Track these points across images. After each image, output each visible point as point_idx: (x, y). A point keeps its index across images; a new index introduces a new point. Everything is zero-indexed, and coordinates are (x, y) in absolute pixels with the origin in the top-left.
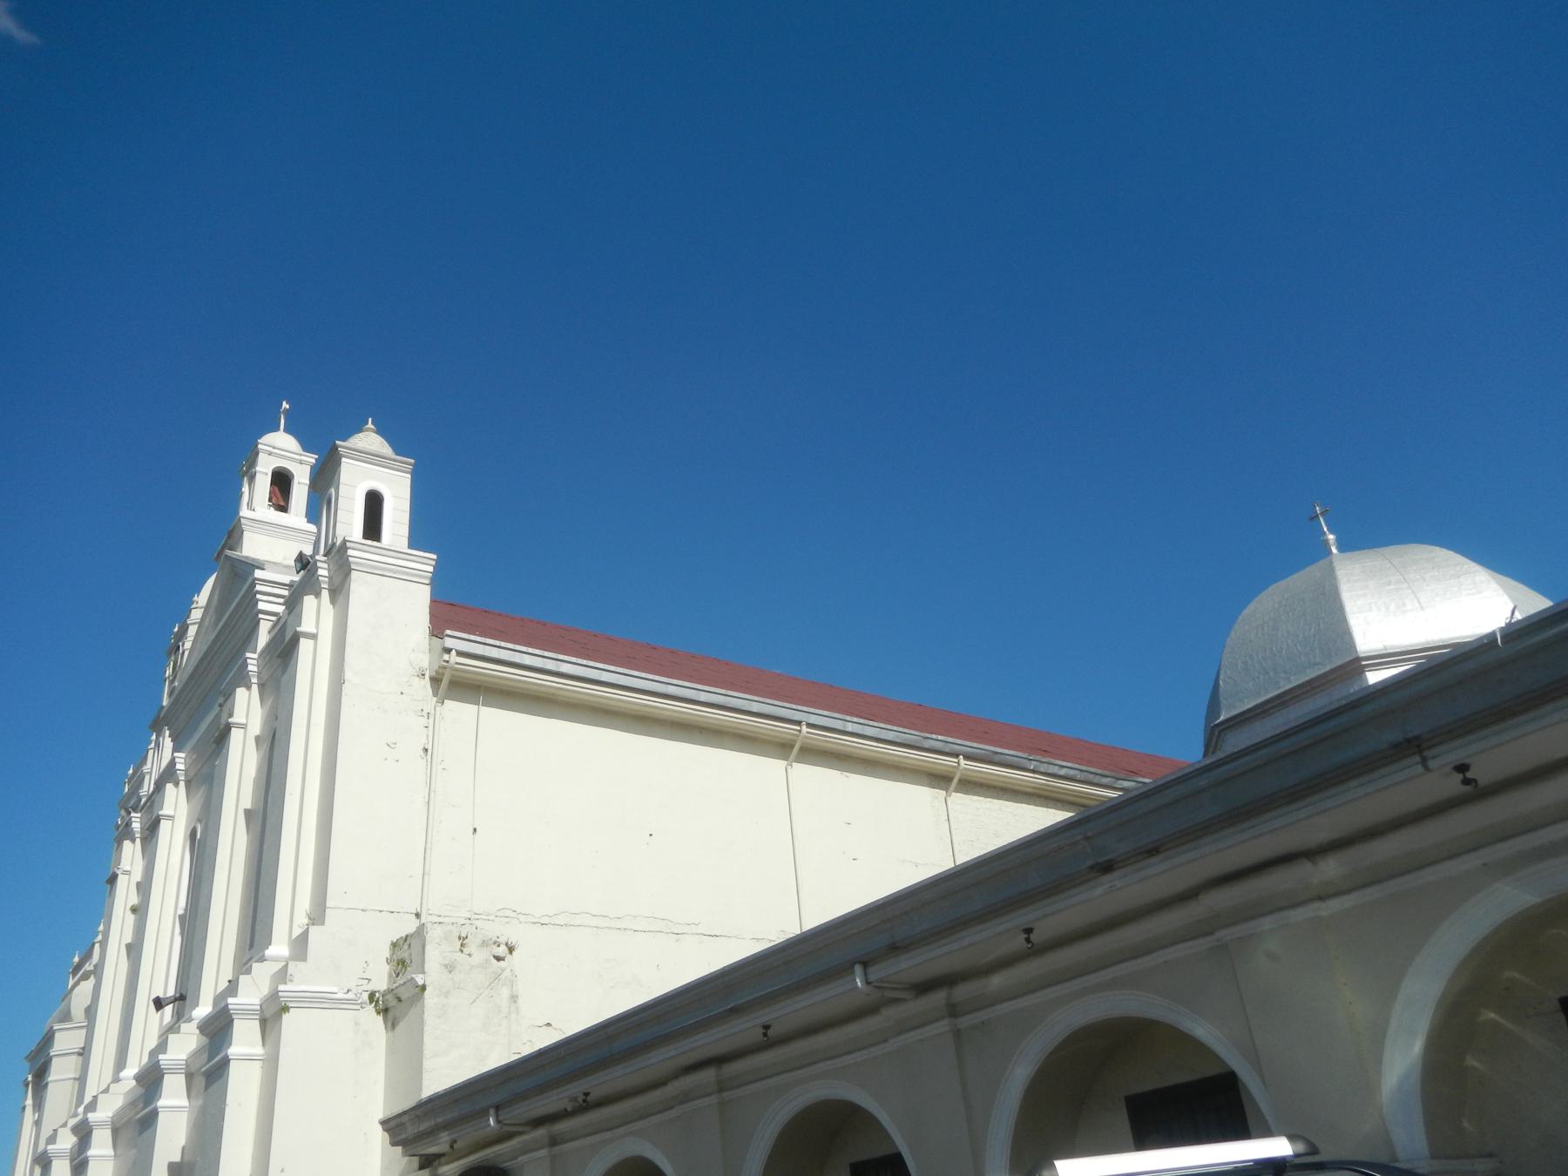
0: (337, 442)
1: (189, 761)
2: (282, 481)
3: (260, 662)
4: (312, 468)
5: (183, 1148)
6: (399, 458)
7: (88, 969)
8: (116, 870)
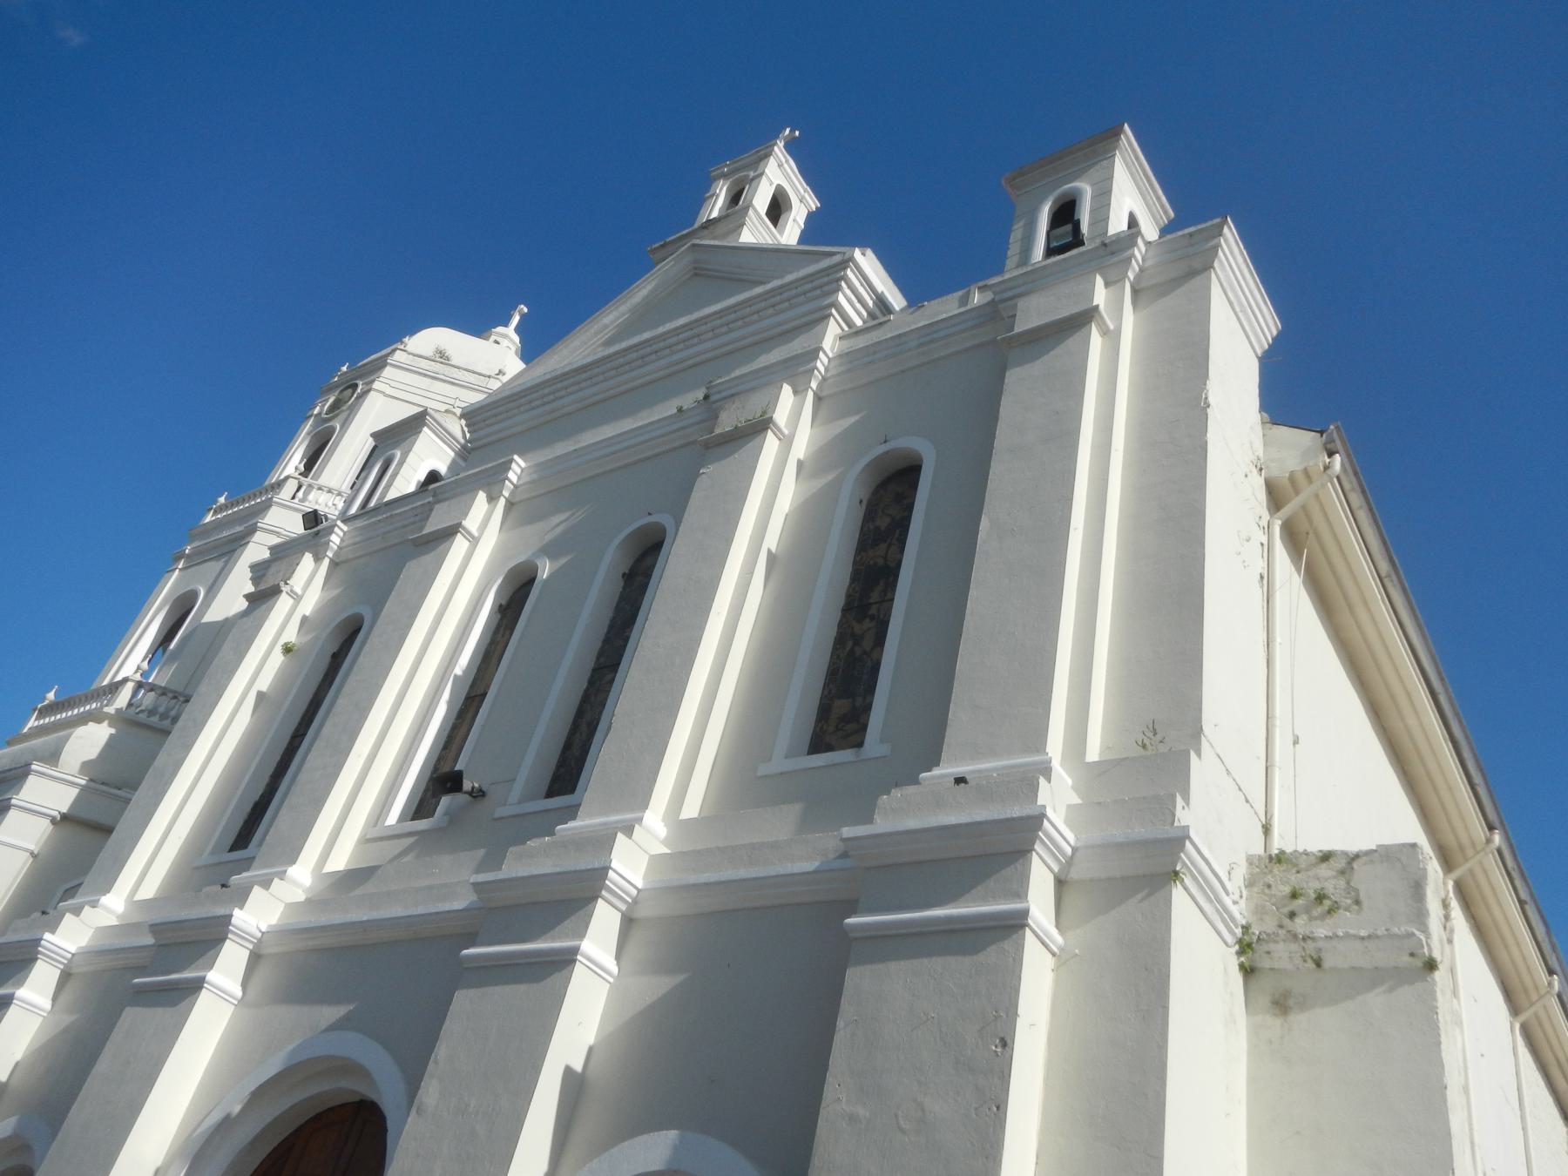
0: (1126, 125)
1: (526, 479)
2: (777, 209)
3: (832, 365)
4: (811, 217)
5: (591, 1050)
6: (1164, 199)
7: (106, 709)
8: (282, 584)
